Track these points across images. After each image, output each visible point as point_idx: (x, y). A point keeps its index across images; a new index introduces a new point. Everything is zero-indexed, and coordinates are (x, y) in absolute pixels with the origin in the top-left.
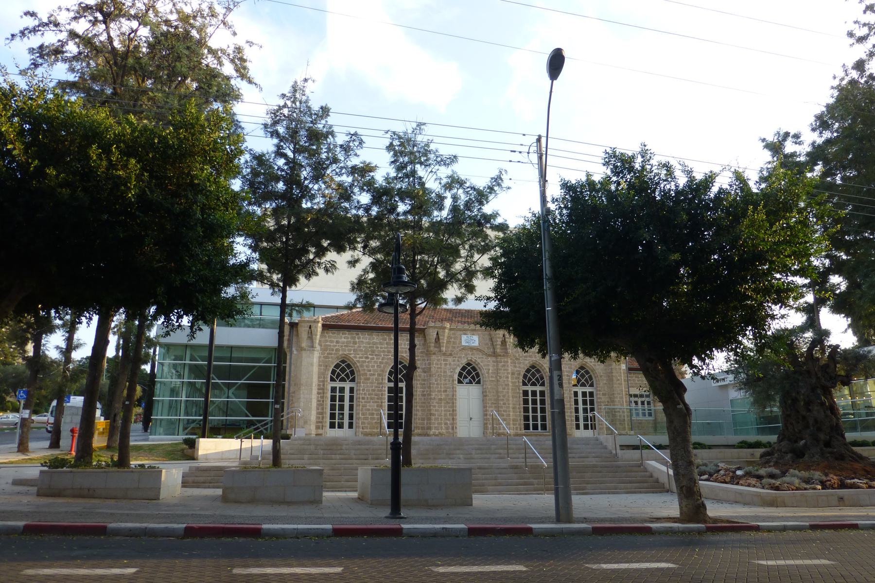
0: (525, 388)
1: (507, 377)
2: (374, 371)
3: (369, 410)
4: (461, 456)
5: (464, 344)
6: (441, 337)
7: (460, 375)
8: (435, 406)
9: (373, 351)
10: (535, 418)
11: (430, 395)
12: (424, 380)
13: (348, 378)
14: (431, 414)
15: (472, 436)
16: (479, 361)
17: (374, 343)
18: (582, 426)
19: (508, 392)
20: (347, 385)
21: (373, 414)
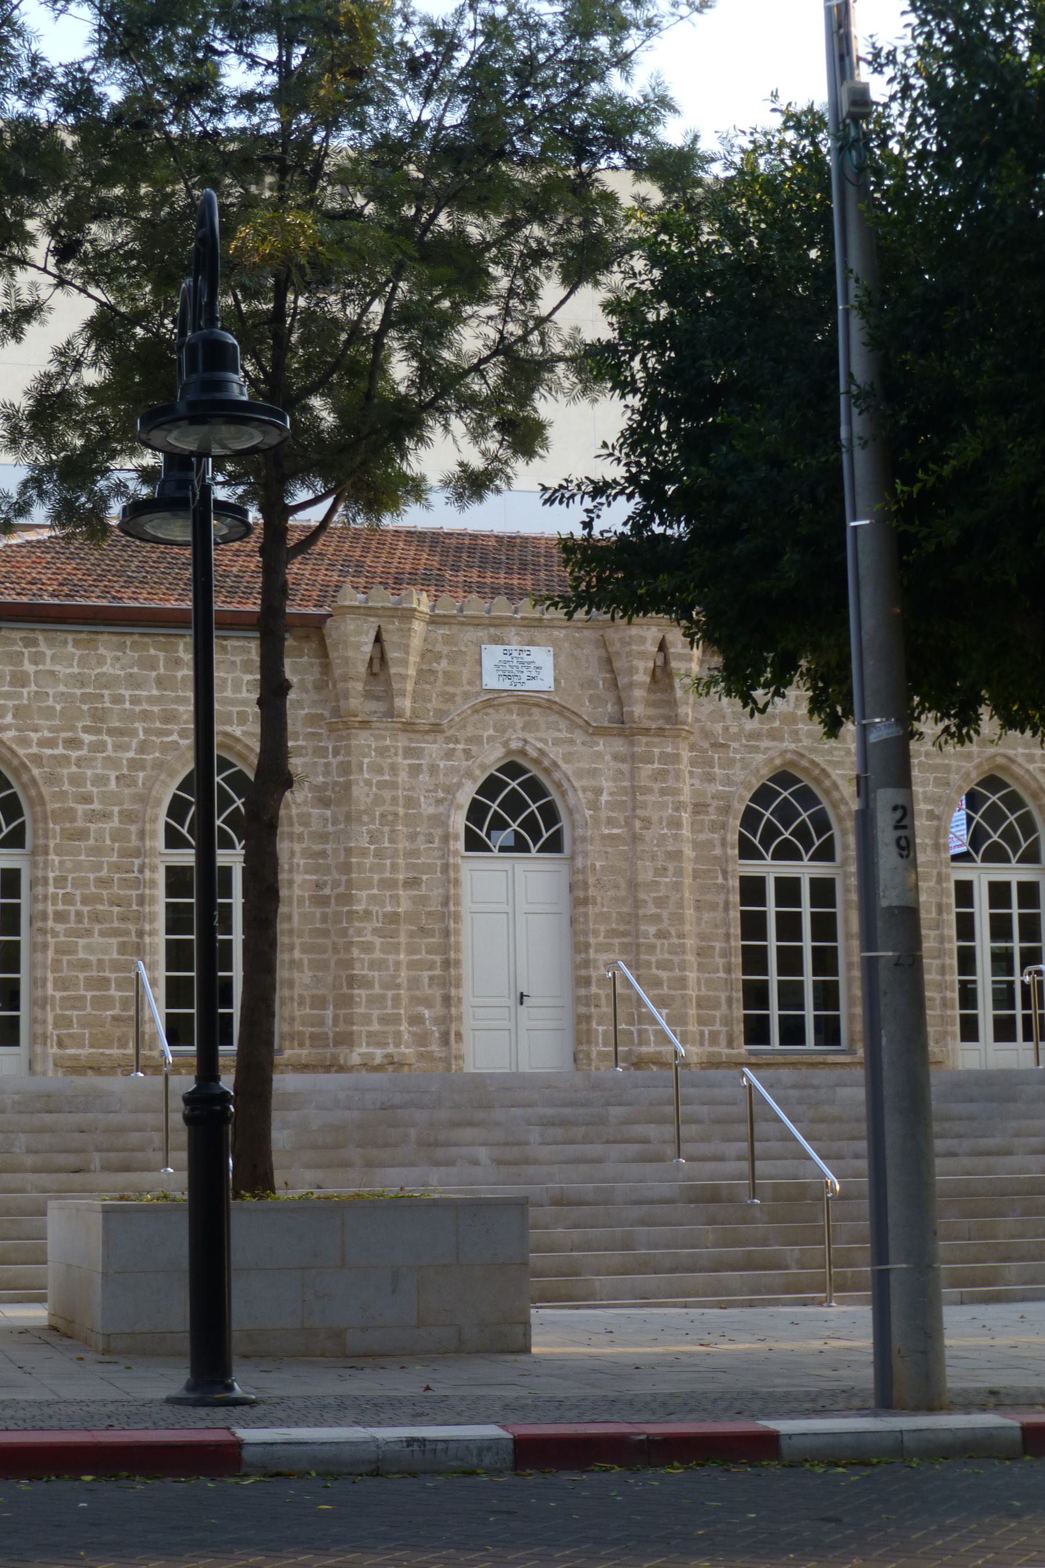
0: (752, 868)
1: (676, 824)
2: (105, 798)
3: (85, 965)
4: (483, 1153)
5: (491, 680)
6: (392, 654)
7: (476, 812)
8: (368, 947)
9: (99, 716)
10: (791, 996)
11: (346, 899)
12: (324, 837)
14: (351, 981)
15: (525, 1068)
16: (555, 753)
17: (105, 682)
18: (986, 1027)
19: (677, 887)
21: (103, 983)
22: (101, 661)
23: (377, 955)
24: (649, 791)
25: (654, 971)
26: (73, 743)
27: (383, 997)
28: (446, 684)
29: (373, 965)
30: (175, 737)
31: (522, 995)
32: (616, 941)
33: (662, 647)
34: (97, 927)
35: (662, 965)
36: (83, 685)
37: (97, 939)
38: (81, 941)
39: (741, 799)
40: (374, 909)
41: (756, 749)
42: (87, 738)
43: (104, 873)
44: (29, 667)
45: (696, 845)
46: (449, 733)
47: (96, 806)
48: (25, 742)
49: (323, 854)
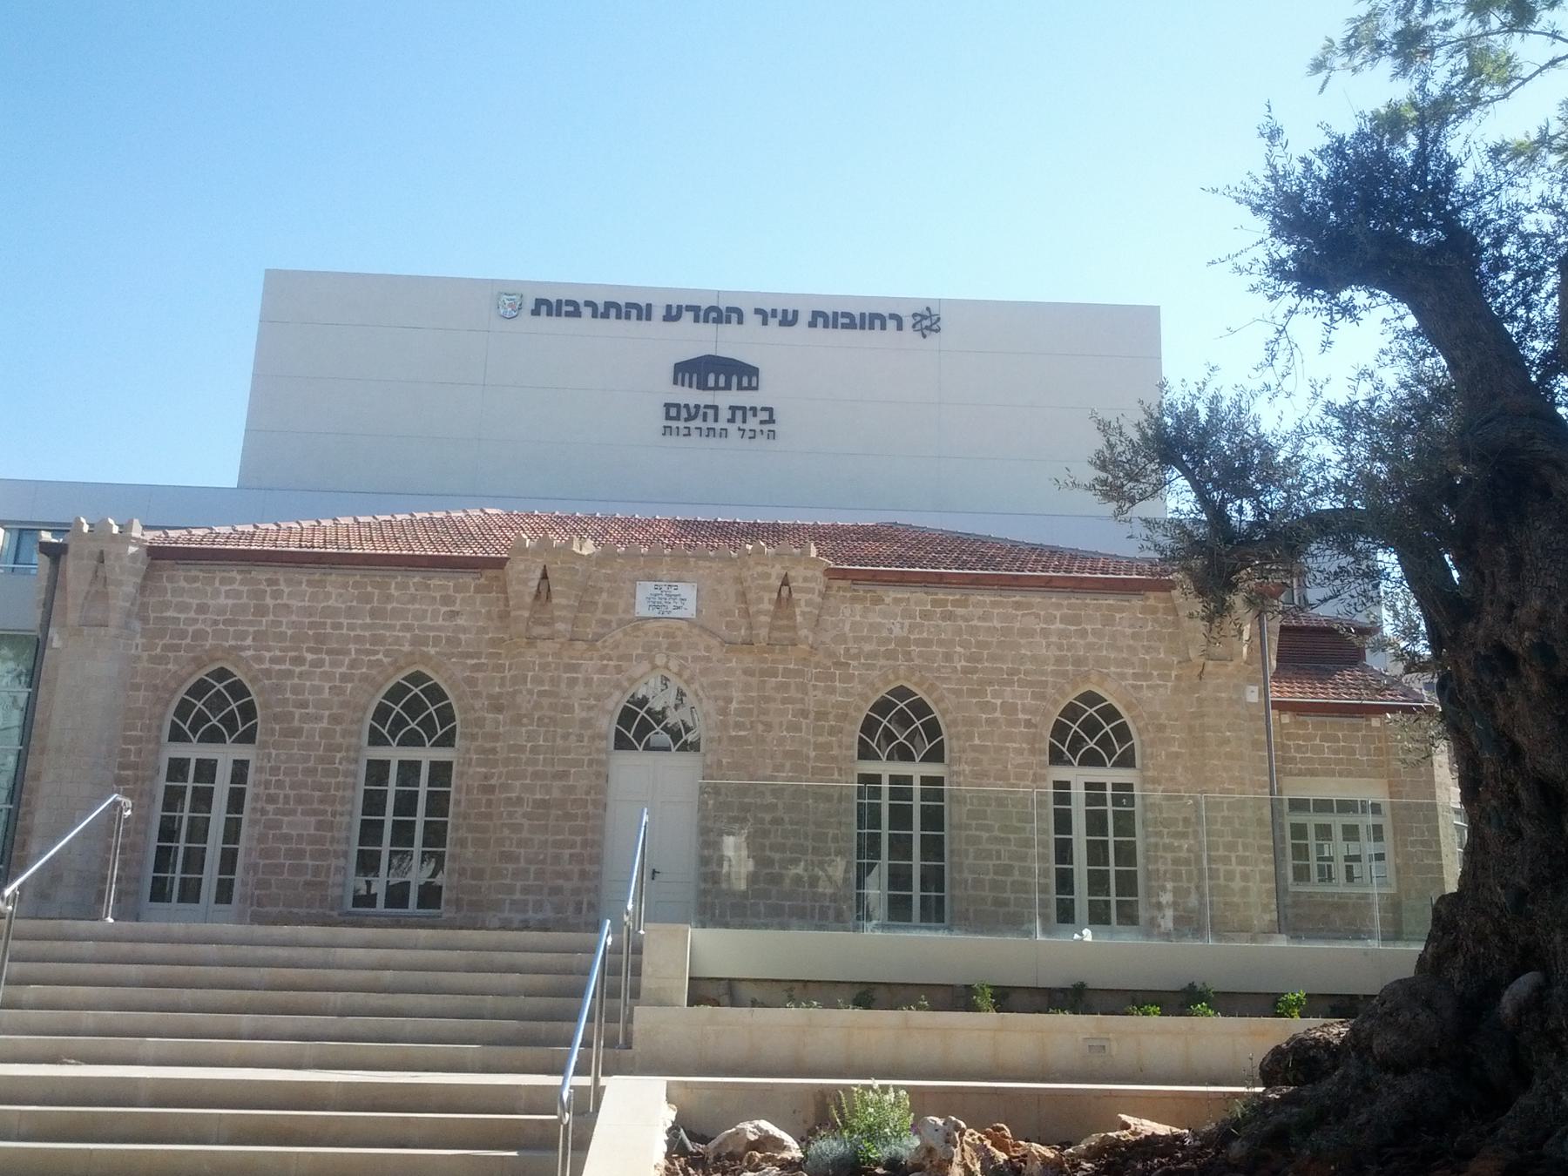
3: (286, 838)
5: (642, 610)
8: (516, 828)
9: (321, 639)
13: (232, 729)
20: (225, 755)
21: (300, 854)
22: (328, 596)
23: (525, 834)
24: (774, 700)
25: (768, 853)
26: (299, 661)
27: (527, 871)
28: (605, 612)
29: (520, 843)
30: (380, 656)
31: (654, 872)
33: (785, 582)
34: (300, 808)
36: (311, 615)
37: (299, 817)
39: (858, 709)
40: (525, 796)
42: (309, 656)
43: (311, 764)
44: (269, 601)
45: (817, 746)
46: (604, 652)
47: (311, 710)
48: (260, 659)
49: (493, 751)
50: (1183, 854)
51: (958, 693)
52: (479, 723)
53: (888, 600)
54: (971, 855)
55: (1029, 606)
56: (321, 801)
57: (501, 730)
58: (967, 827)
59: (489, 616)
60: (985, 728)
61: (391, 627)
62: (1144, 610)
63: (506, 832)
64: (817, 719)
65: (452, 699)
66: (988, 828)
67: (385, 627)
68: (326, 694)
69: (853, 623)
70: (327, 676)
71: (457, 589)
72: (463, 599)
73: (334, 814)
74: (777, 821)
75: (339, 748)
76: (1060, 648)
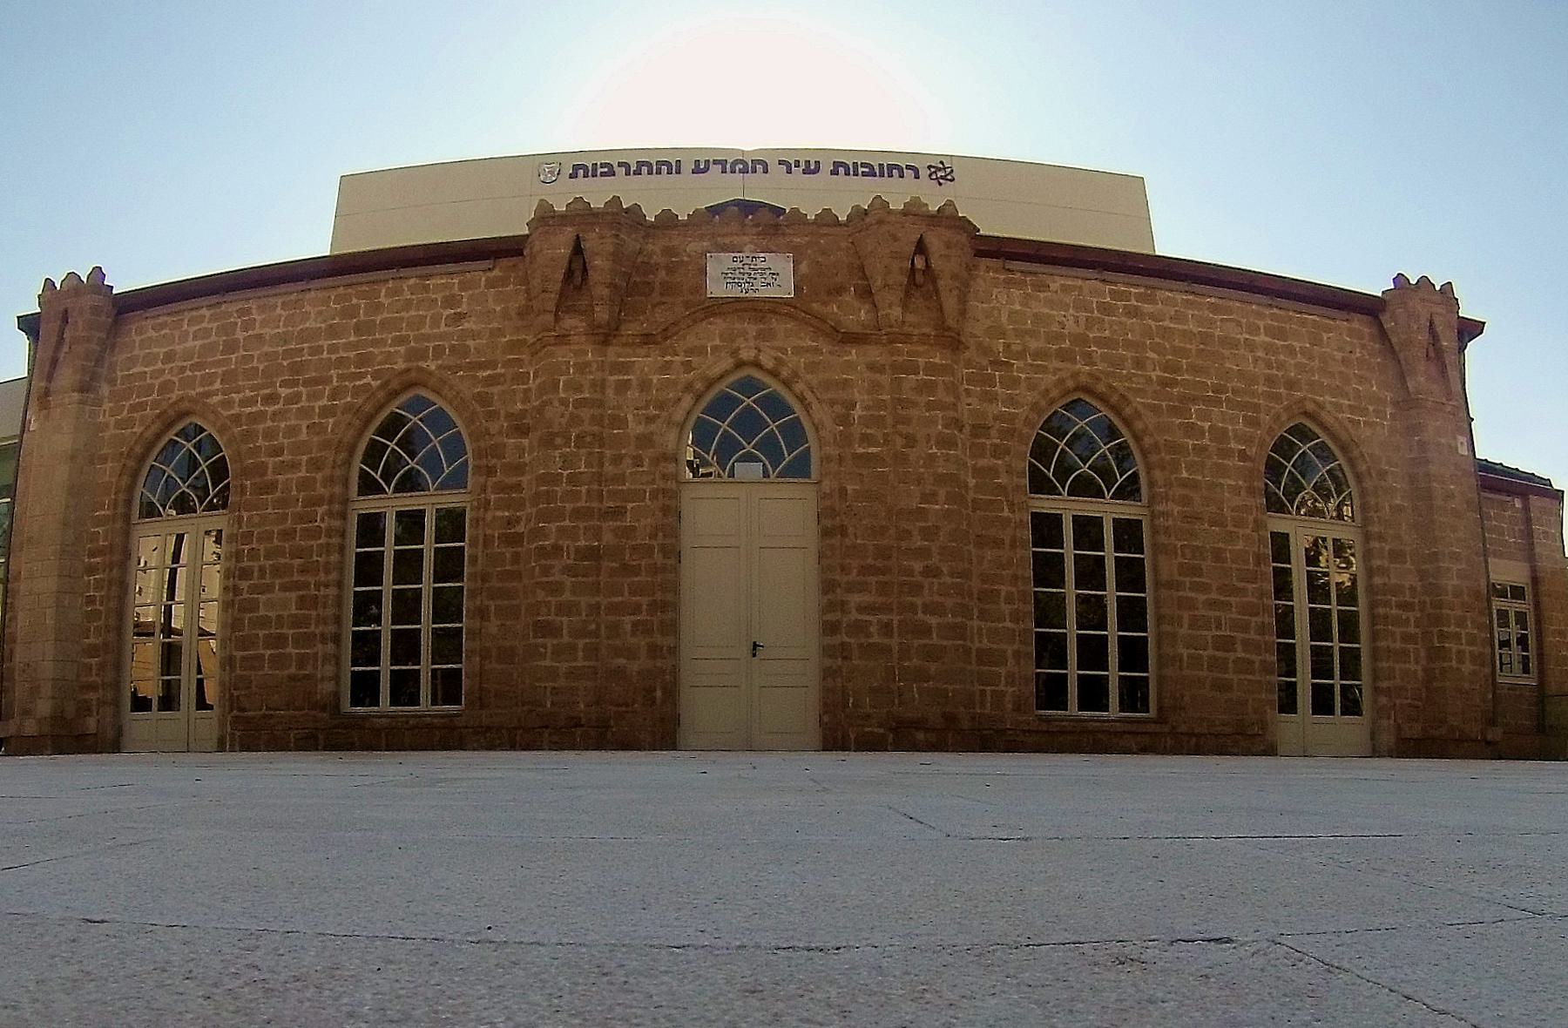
2: (298, 448)
9: (296, 369)
22: (305, 317)
23: (567, 596)
25: (920, 615)
27: (573, 648)
31: (755, 645)
32: (873, 579)
35: (929, 609)
37: (278, 595)
38: (262, 598)
41: (1044, 370)
42: (284, 392)
45: (977, 472)
47: (286, 457)
50: (1412, 630)
51: (1155, 409)
52: (497, 451)
53: (1053, 287)
54: (1186, 622)
55: (1229, 311)
56: (303, 571)
57: (527, 458)
58: (1178, 586)
59: (505, 314)
60: (1193, 458)
61: (382, 342)
62: (1351, 332)
63: (541, 595)
64: (974, 435)
65: (461, 427)
66: (1205, 588)
67: (375, 343)
68: (303, 436)
69: (1011, 313)
70: (304, 413)
71: (464, 286)
72: (471, 298)
73: (317, 586)
74: (930, 572)
75: (318, 501)
76: (1269, 366)
